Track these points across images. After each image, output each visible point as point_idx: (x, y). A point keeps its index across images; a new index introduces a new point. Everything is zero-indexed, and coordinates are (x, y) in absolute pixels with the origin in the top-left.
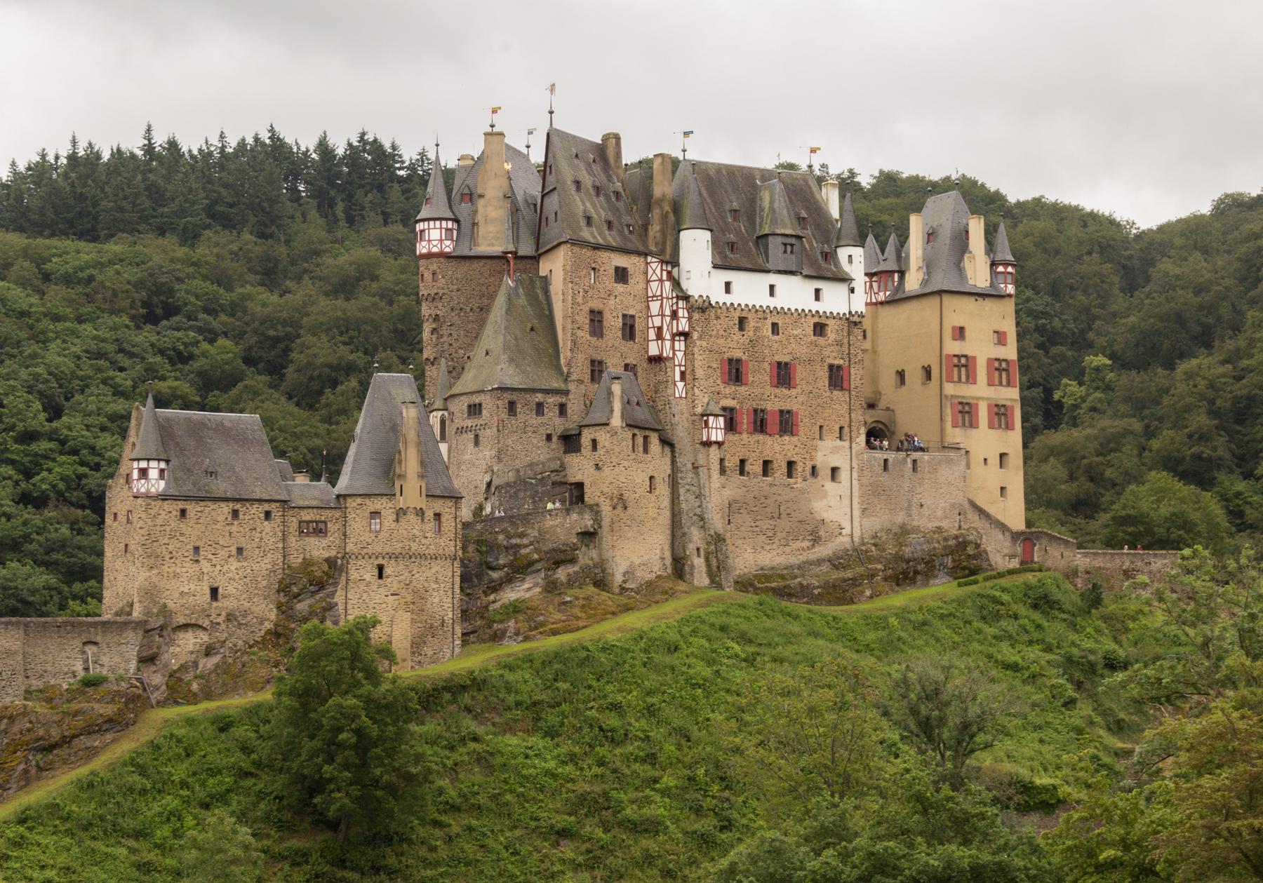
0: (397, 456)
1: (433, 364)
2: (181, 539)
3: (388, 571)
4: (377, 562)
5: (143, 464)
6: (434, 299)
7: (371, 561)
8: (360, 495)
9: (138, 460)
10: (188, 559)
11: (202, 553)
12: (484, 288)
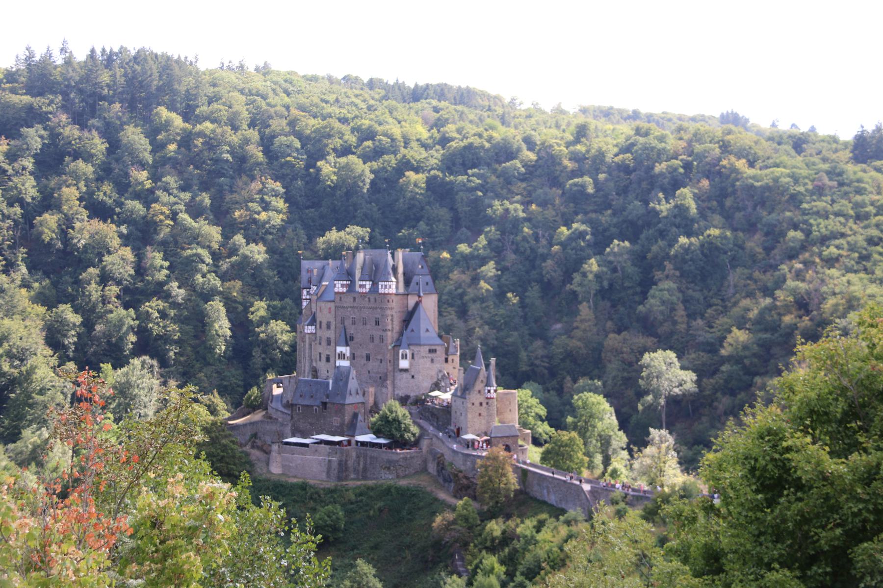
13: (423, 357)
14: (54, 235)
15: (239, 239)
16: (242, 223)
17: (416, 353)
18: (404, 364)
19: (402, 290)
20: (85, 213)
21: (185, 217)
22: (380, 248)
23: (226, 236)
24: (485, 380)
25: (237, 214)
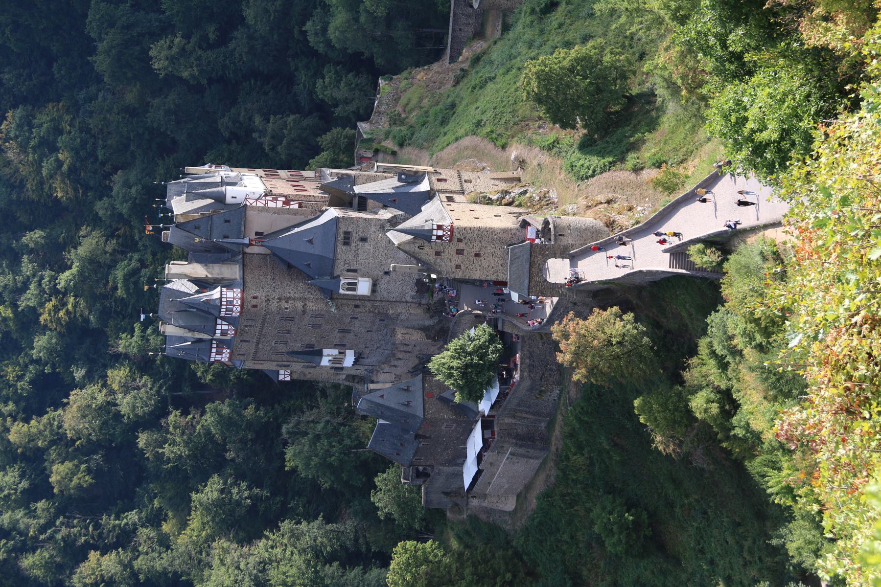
3: (467, 178)
5: (435, 227)
6: (268, 300)
12: (261, 278)
13: (356, 256)
14: (83, 467)
15: (101, 208)
16: (76, 190)
17: (347, 266)
18: (364, 287)
19: (232, 271)
20: (51, 414)
21: (64, 278)
22: (158, 295)
23: (96, 222)
24: (420, 242)
25: (60, 195)
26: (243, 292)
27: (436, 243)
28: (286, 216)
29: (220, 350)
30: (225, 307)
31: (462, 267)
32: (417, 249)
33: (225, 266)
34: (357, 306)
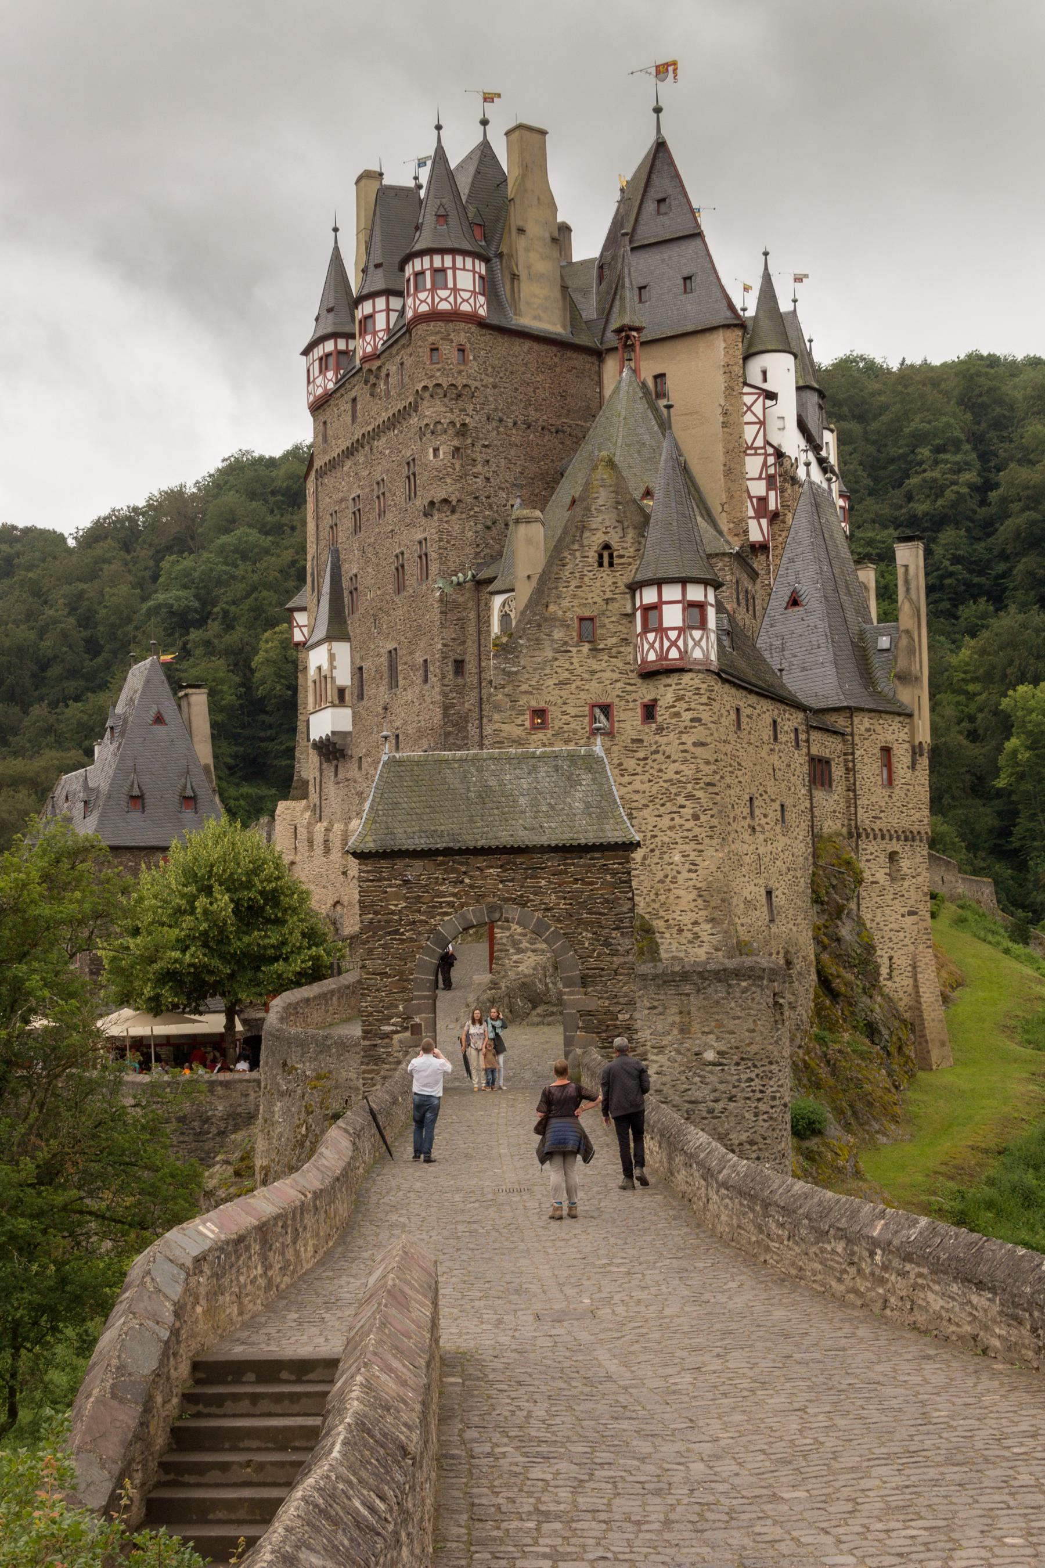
0: (904, 641)
1: (453, 512)
2: (740, 773)
3: (905, 864)
4: (890, 849)
5: (695, 593)
6: (459, 396)
7: (884, 844)
8: (870, 711)
9: (684, 582)
10: (745, 823)
11: (757, 812)
26: (482, 324)
27: (631, 616)
28: (720, 448)
29: (332, 361)
30: (427, 265)
31: (540, 735)
32: (599, 538)
33: (557, 294)
34: (459, 666)
